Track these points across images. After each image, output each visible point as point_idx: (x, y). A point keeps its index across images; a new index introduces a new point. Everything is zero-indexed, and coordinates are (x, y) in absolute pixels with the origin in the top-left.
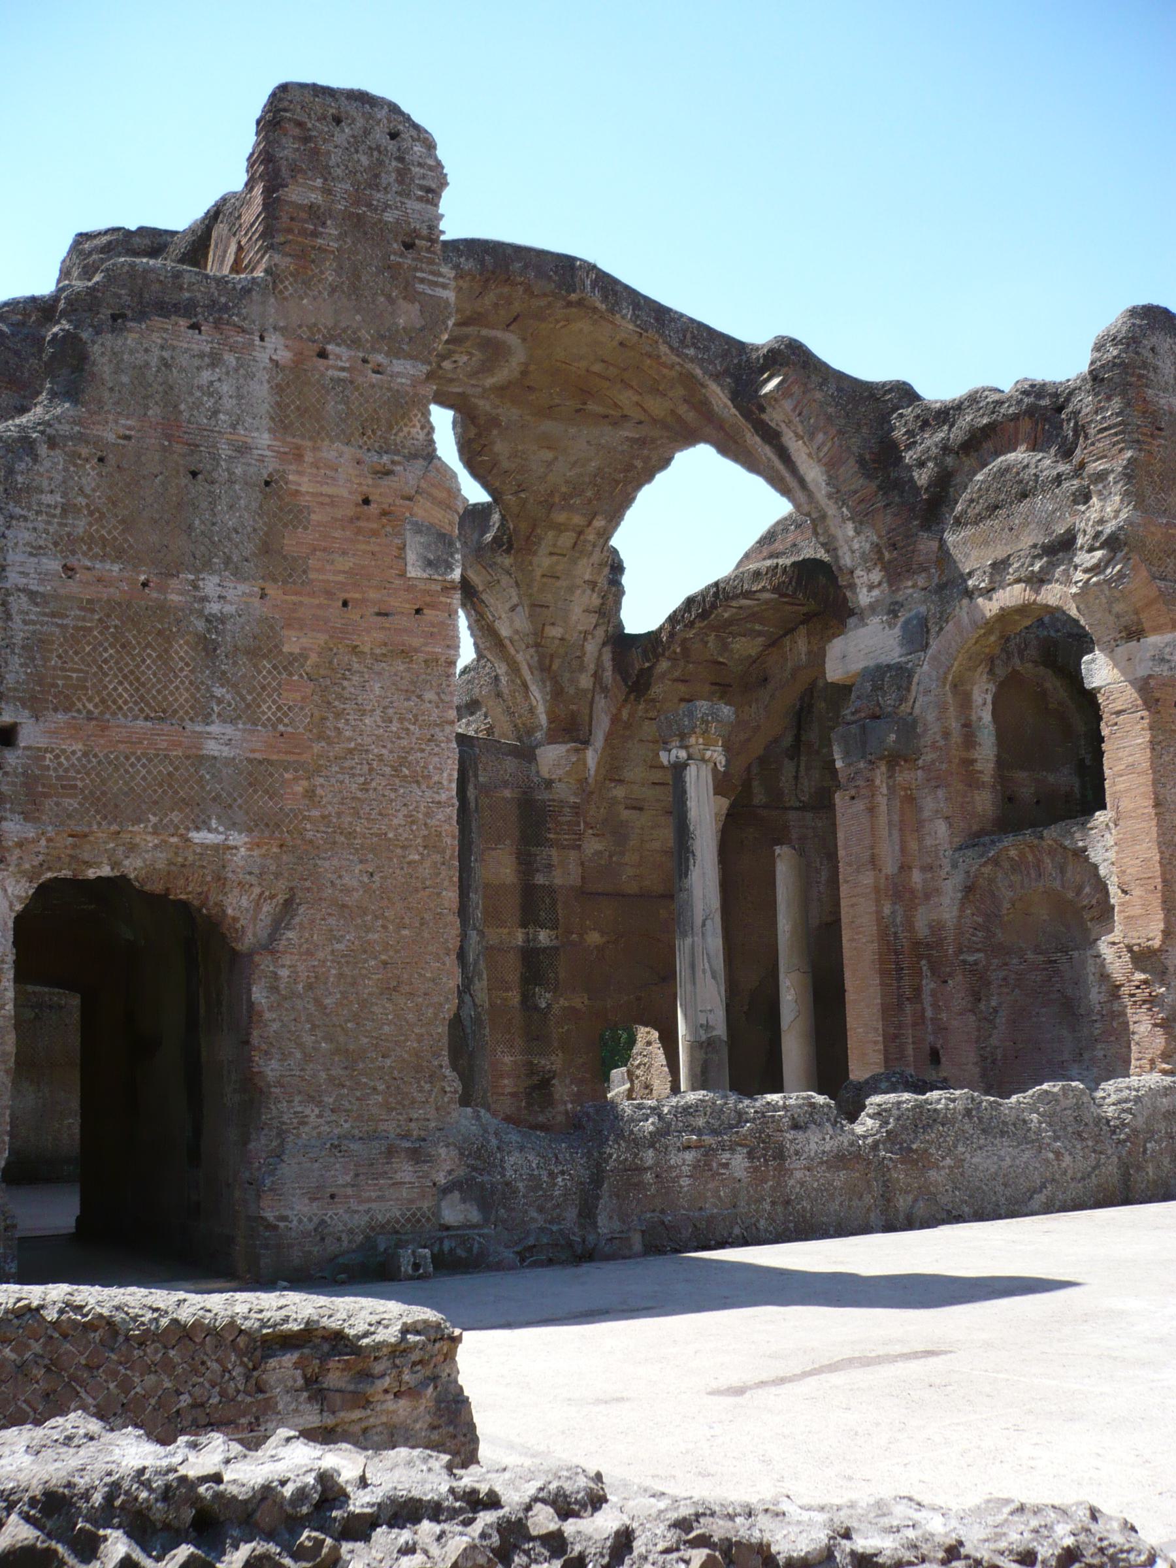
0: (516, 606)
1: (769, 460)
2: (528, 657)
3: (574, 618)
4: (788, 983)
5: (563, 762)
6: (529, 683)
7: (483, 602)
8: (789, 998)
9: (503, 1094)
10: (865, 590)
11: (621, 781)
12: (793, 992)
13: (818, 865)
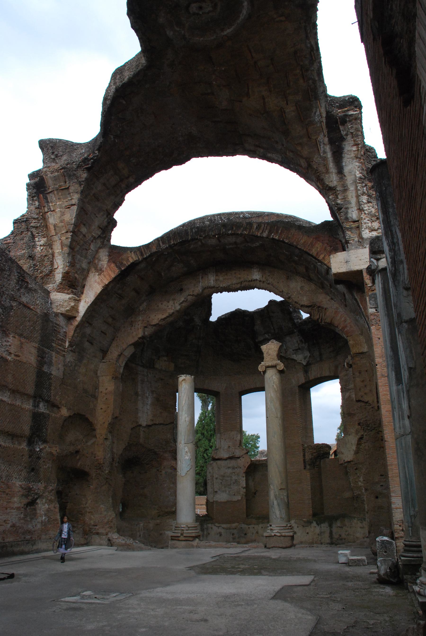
0: (74, 205)
1: (325, 152)
2: (64, 238)
3: (93, 227)
4: (187, 449)
5: (66, 304)
6: (56, 255)
7: (46, 198)
8: (187, 458)
9: (12, 508)
10: (367, 231)
11: (90, 324)
12: (189, 454)
13: (148, 395)
